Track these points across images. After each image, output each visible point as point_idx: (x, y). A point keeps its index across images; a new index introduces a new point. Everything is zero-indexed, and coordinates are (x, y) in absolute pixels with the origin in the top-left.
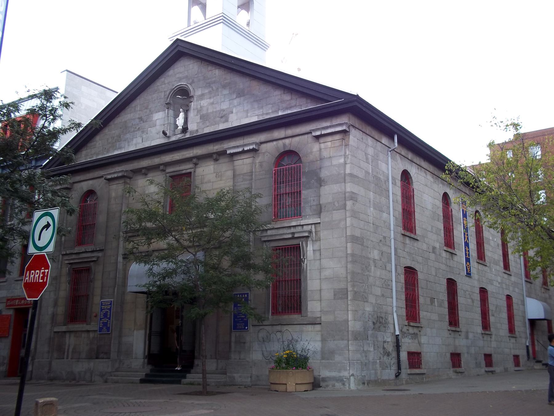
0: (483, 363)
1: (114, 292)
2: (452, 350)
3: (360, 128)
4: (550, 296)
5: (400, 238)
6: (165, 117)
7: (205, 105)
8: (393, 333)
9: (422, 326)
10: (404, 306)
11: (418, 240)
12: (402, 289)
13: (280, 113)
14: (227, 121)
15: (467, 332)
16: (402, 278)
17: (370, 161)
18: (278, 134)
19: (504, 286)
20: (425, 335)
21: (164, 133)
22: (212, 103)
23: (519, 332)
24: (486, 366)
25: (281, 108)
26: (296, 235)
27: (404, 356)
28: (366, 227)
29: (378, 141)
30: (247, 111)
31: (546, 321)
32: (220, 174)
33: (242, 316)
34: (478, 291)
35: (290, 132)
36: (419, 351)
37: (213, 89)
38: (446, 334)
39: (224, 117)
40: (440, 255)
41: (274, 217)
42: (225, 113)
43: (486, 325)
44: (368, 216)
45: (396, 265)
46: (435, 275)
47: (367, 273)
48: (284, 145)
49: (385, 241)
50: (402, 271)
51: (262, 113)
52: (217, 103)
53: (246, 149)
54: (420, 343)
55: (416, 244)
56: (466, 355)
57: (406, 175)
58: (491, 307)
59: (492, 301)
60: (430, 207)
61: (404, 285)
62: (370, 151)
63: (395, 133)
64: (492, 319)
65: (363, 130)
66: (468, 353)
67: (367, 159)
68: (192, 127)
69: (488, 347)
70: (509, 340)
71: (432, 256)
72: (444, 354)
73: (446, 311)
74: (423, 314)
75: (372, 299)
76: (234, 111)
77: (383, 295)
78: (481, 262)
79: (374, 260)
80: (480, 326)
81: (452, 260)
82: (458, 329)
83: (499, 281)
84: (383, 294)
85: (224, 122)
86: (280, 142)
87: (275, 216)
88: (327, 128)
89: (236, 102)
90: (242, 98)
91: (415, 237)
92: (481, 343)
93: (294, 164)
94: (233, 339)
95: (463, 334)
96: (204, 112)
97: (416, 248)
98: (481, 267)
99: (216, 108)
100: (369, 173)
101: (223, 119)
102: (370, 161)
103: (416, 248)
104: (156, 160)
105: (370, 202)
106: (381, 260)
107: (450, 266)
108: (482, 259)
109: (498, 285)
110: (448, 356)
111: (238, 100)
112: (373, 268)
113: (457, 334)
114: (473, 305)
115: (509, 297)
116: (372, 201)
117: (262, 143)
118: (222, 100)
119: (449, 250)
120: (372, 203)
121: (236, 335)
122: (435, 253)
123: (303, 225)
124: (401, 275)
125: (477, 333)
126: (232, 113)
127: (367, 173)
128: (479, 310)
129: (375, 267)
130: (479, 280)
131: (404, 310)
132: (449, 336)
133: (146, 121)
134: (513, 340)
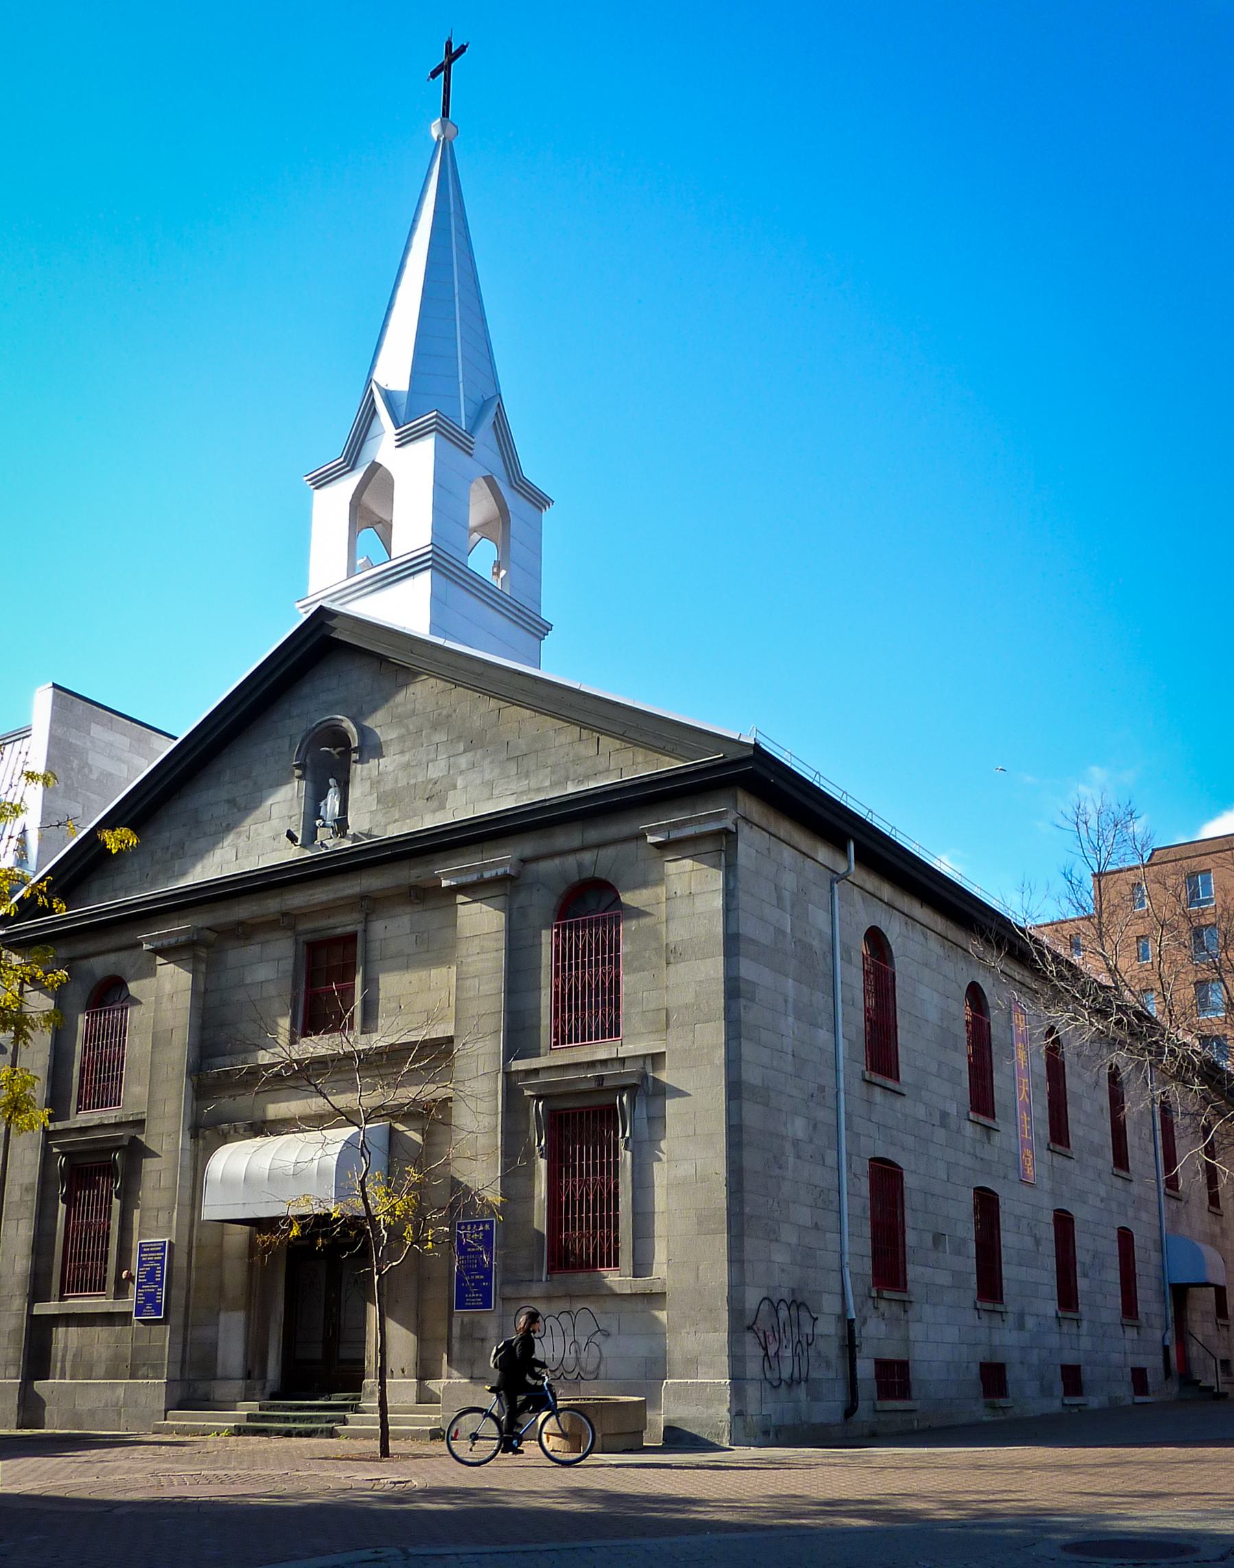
0: (1059, 1387)
1: (171, 1217)
2: (982, 1355)
3: (764, 823)
4: (1224, 1232)
5: (859, 1088)
6: (292, 800)
7: (390, 768)
8: (839, 1317)
9: (912, 1299)
10: (868, 1250)
11: (904, 1095)
12: (865, 1213)
13: (571, 789)
14: (442, 807)
15: (1021, 1317)
16: (865, 1187)
17: (788, 904)
18: (564, 839)
19: (1114, 1206)
20: (918, 1321)
21: (291, 836)
22: (407, 766)
23: (1146, 1314)
25: (572, 777)
26: (607, 1084)
27: (866, 1369)
29: (809, 857)
30: (490, 785)
31: (1213, 1289)
32: (425, 935)
33: (477, 1277)
34: (1049, 1218)
35: (594, 834)
37: (408, 730)
38: (971, 1317)
39: (436, 798)
40: (958, 1132)
41: (553, 1040)
42: (438, 787)
43: (1067, 1297)
44: (783, 1035)
45: (849, 1155)
46: (945, 1178)
48: (580, 865)
50: (863, 1168)
51: (526, 788)
52: (419, 764)
53: (487, 875)
54: (906, 1340)
55: (898, 1103)
57: (875, 938)
58: (1081, 1256)
59: (1081, 1240)
60: (933, 1016)
62: (789, 881)
63: (848, 837)
64: (1082, 1284)
65: (772, 830)
66: (1022, 1363)
67: (780, 899)
68: (357, 822)
69: (1072, 1349)
70: (1121, 1330)
71: (940, 1135)
72: (965, 1364)
73: (971, 1265)
74: (914, 1272)
75: (789, 1235)
76: (460, 783)
77: (816, 1227)
78: (1059, 1148)
79: (796, 1143)
80: (1054, 1300)
81: (989, 1142)
82: (999, 1308)
83: (1103, 1193)
84: (816, 1223)
85: (434, 811)
86: (571, 861)
87: (556, 1036)
88: (683, 824)
89: (463, 761)
90: (480, 752)
91: (897, 1087)
92: (1053, 1340)
93: (604, 912)
94: (456, 1330)
95: (1010, 1318)
96: (389, 787)
97: (899, 1115)
98: (1058, 1160)
99: (415, 776)
100: (784, 933)
101: (435, 804)
102: (788, 904)
103: (899, 1115)
104: (272, 905)
105: (786, 1002)
106: (811, 1141)
107: (982, 1159)
108: (1060, 1143)
109: (1098, 1204)
110: (975, 1370)
111: (469, 755)
112: (791, 1160)
113: (997, 1317)
114: (1038, 1250)
115: (1125, 1237)
116: (790, 1000)
117: (524, 861)
118: (432, 756)
119: (983, 1119)
120: (790, 1005)
121: (462, 1321)
122: (945, 1127)
123: (622, 1060)
124: (862, 1178)
125: (1045, 1316)
126: (455, 787)
127: (779, 932)
128: (1052, 1263)
129: (799, 1157)
130: (1053, 1193)
131: (868, 1263)
132: (978, 1323)
133: (246, 809)
134: (1131, 1333)
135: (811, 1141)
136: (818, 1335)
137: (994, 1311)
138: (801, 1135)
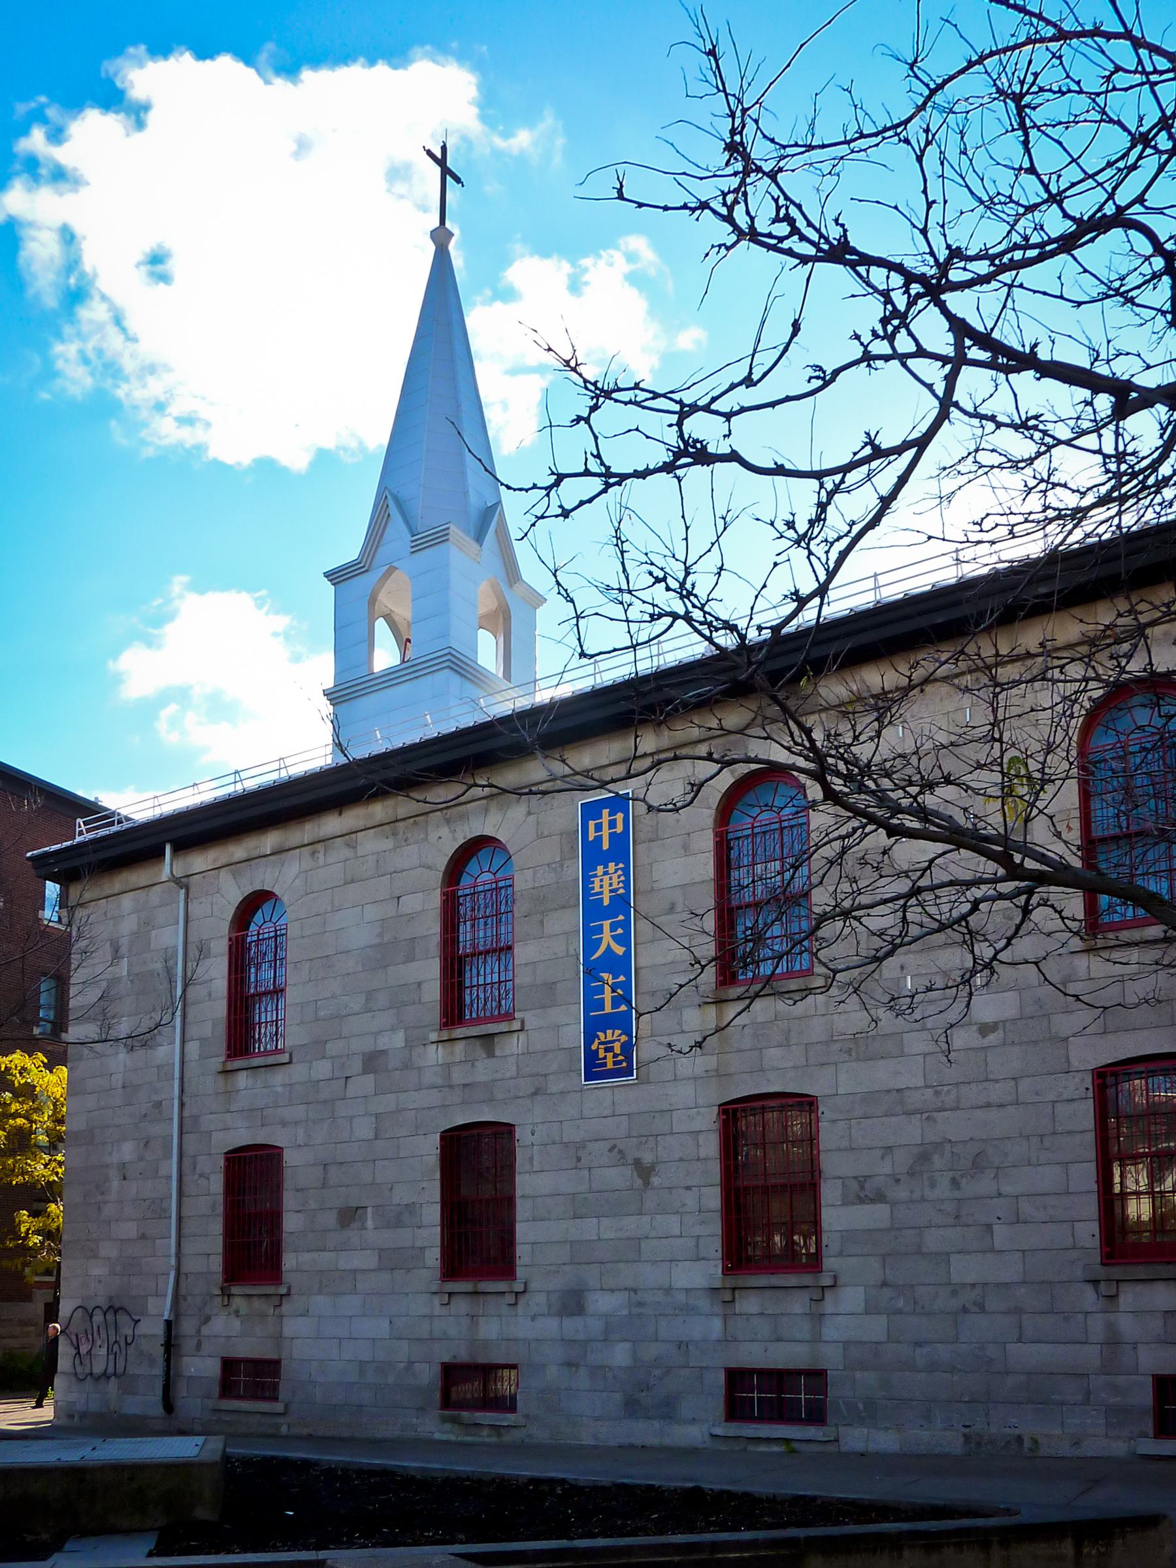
24: (735, 1410)
28: (103, 1104)
36: (272, 1355)
47: (100, 1198)
49: (160, 1112)
54: (279, 1338)
55: (279, 1078)
56: (552, 1372)
61: (220, 1199)
74: (289, 1261)
75: (108, 1250)
77: (143, 1237)
95: (537, 1301)
97: (279, 1089)
103: (279, 1089)
110: (428, 1375)
112: (115, 1184)
132: (438, 1310)
135: (141, 1158)
136: (140, 1336)
137: (476, 1293)
138: (127, 1158)
